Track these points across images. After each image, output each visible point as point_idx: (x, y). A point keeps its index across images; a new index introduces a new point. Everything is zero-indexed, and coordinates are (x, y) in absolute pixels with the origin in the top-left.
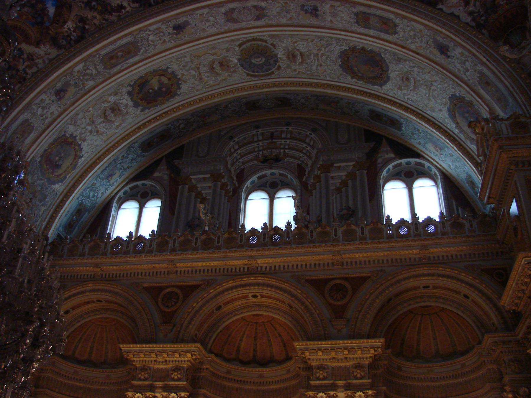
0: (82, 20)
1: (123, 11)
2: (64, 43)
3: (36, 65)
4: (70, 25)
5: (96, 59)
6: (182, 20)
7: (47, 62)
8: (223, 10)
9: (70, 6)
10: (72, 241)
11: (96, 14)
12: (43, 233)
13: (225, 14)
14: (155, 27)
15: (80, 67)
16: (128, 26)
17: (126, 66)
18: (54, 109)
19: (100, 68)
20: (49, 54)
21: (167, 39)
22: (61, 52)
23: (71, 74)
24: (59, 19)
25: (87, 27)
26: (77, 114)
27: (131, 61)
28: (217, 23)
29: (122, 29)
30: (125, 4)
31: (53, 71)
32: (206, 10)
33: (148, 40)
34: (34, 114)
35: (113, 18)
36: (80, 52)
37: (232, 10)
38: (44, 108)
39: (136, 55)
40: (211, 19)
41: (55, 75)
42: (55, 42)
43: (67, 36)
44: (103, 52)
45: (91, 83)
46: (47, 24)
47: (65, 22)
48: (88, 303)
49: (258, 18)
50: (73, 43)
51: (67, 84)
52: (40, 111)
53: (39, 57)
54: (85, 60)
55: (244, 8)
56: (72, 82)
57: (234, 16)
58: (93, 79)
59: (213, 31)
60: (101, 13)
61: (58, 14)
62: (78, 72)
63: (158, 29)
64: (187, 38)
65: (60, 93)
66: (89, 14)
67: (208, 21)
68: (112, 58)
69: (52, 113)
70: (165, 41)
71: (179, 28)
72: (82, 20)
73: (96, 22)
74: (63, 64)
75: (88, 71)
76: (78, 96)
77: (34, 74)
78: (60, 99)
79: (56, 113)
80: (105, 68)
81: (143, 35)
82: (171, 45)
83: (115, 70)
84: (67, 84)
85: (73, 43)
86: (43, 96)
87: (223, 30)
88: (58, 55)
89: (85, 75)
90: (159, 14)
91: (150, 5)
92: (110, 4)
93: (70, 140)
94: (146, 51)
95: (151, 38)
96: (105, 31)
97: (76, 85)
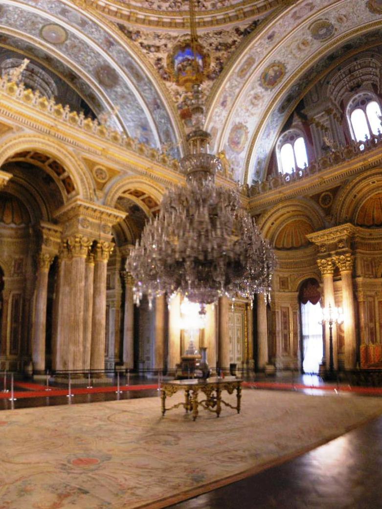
0: (218, 59)
1: (237, 43)
2: (214, 75)
3: (205, 94)
4: (213, 64)
5: (234, 76)
6: (270, 33)
7: (210, 90)
8: (290, 15)
9: (208, 55)
10: (262, 183)
11: (223, 52)
12: (244, 183)
13: (292, 17)
14: (258, 43)
15: (228, 85)
16: (243, 50)
17: (251, 71)
18: (224, 113)
19: (238, 79)
20: (209, 85)
21: (267, 46)
22: (215, 81)
23: (225, 91)
24: (206, 64)
25: (222, 61)
26: (237, 110)
27: (253, 68)
28: (290, 23)
29: (241, 53)
30: (236, 39)
31: (214, 95)
32: (281, 21)
33: (257, 52)
34: (215, 122)
35: (233, 49)
36: (224, 77)
37: (295, 13)
38: (219, 116)
39: (254, 62)
40: (286, 23)
41: (217, 96)
42: (209, 77)
43: (214, 71)
44: (237, 71)
45: (237, 90)
46: (201, 70)
47: (209, 65)
48: (283, 215)
49: (311, 10)
50: (218, 73)
51: (225, 97)
52: (217, 119)
53: (205, 89)
54: (229, 80)
55: (301, 9)
56: (227, 95)
57: (298, 15)
58: (238, 87)
59: (290, 29)
60: (226, 50)
61: (204, 62)
62: (228, 87)
63: (260, 43)
64: (278, 40)
65: (224, 104)
66: (219, 54)
67: (285, 25)
68: (242, 71)
69: (224, 116)
70: (267, 48)
71: (270, 37)
72: (218, 59)
73: (225, 56)
74: (218, 87)
75: (233, 85)
76: (234, 100)
77: (206, 100)
78: (225, 106)
79: (226, 115)
80: (241, 78)
81: (254, 51)
82: (271, 48)
83: (247, 76)
84: (225, 97)
85: (218, 73)
86: (216, 110)
87: (295, 26)
88: (214, 84)
89: (232, 87)
90: (256, 36)
91: (249, 33)
92: (228, 43)
93: (239, 126)
94: (259, 59)
95: (258, 50)
96: (232, 59)
97: (230, 95)
